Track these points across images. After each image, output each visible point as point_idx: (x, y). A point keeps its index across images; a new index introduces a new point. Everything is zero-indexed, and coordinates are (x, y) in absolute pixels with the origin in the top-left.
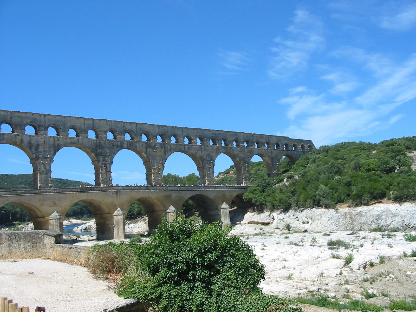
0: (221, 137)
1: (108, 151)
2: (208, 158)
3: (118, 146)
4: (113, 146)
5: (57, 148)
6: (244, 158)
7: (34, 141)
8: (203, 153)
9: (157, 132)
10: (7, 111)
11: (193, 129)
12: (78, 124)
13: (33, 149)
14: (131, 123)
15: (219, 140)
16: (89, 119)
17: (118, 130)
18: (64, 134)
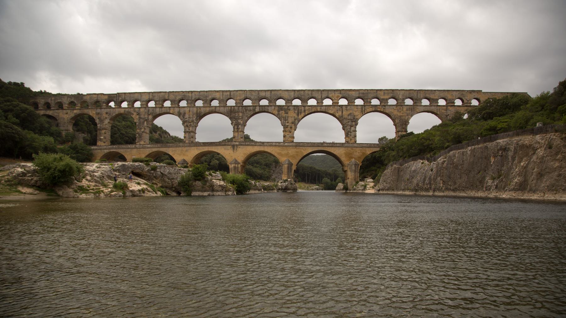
0: (371, 96)
1: (241, 114)
2: (349, 117)
3: (250, 110)
4: (246, 110)
5: (200, 116)
6: (400, 116)
7: (182, 111)
8: (344, 112)
9: (292, 97)
10: (166, 92)
11: (335, 90)
12: (217, 96)
13: (181, 117)
14: (265, 91)
15: (367, 99)
16: (227, 91)
17: (252, 97)
18: (206, 105)
